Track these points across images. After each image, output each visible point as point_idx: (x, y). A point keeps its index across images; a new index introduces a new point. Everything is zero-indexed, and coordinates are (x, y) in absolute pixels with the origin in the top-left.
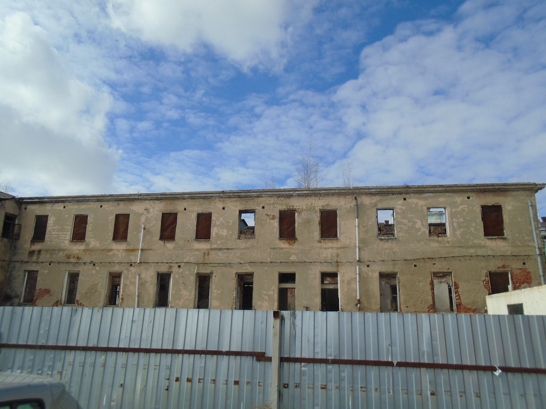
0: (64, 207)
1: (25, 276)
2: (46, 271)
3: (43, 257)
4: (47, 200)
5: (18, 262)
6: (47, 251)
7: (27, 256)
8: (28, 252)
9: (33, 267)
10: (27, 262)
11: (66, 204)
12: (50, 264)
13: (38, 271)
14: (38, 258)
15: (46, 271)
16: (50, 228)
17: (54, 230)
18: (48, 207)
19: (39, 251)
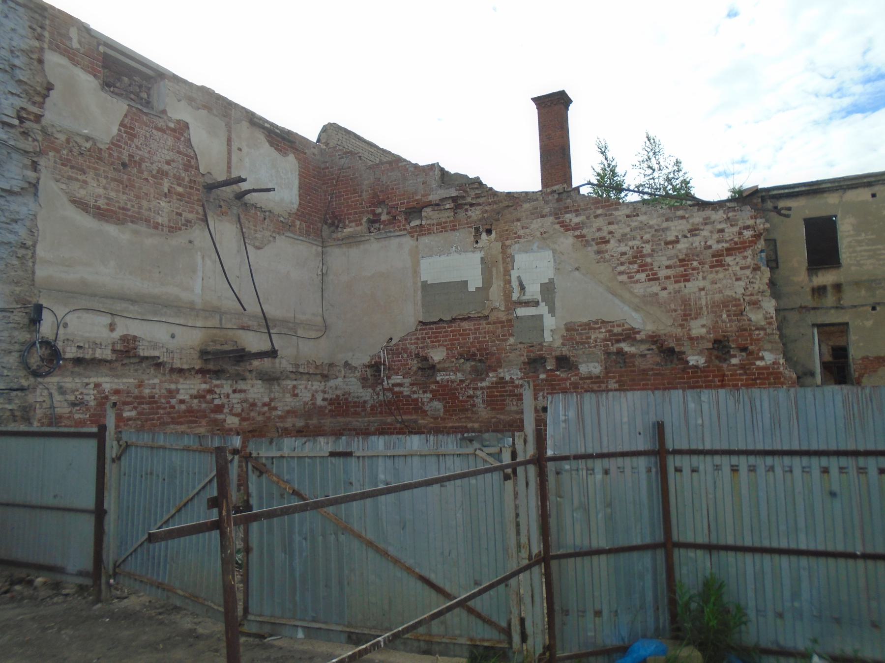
0: (874, 195)
1: (813, 334)
2: (869, 324)
3: (849, 297)
4: (829, 185)
5: (792, 309)
6: (857, 284)
7: (810, 298)
8: (808, 289)
9: (834, 317)
10: (814, 309)
11: (876, 189)
12: (874, 309)
13: (847, 324)
14: (839, 299)
15: (869, 324)
16: (849, 239)
17: (859, 242)
18: (832, 199)
19: (838, 287)
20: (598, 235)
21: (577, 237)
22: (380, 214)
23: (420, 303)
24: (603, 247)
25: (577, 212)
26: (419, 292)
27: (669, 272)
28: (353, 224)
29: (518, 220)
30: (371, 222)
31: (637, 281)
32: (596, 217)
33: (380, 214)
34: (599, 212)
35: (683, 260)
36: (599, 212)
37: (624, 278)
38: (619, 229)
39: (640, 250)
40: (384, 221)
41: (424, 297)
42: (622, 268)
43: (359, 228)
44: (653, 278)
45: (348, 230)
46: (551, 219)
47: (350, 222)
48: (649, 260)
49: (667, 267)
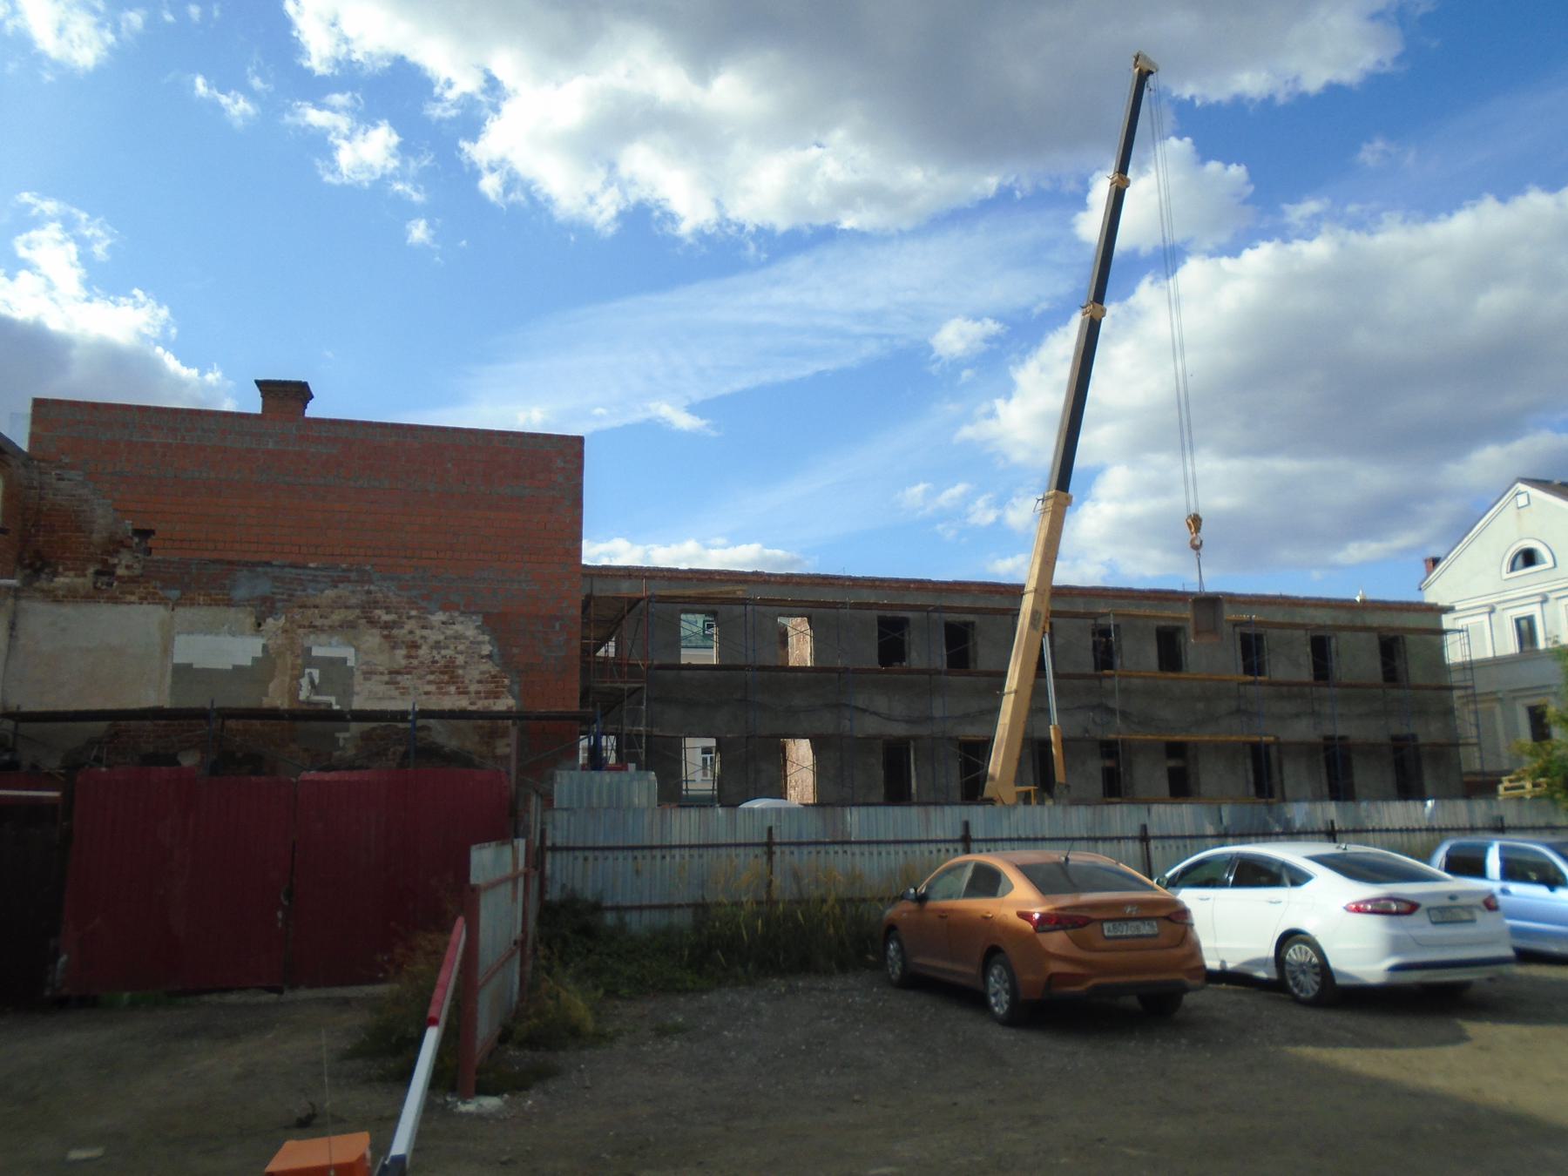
20: (410, 637)
21: (385, 637)
22: (115, 566)
23: (167, 691)
24: (413, 653)
25: (388, 610)
26: (168, 680)
27: (481, 687)
28: (72, 573)
29: (316, 607)
30: (98, 573)
31: (447, 693)
32: (409, 618)
33: (115, 566)
34: (413, 613)
35: (494, 677)
36: (413, 613)
37: (432, 688)
38: (434, 636)
39: (452, 660)
40: (119, 578)
41: (174, 683)
42: (431, 677)
43: (80, 580)
44: (463, 692)
45: (60, 581)
46: (358, 612)
47: (66, 569)
48: (460, 672)
49: (480, 682)
